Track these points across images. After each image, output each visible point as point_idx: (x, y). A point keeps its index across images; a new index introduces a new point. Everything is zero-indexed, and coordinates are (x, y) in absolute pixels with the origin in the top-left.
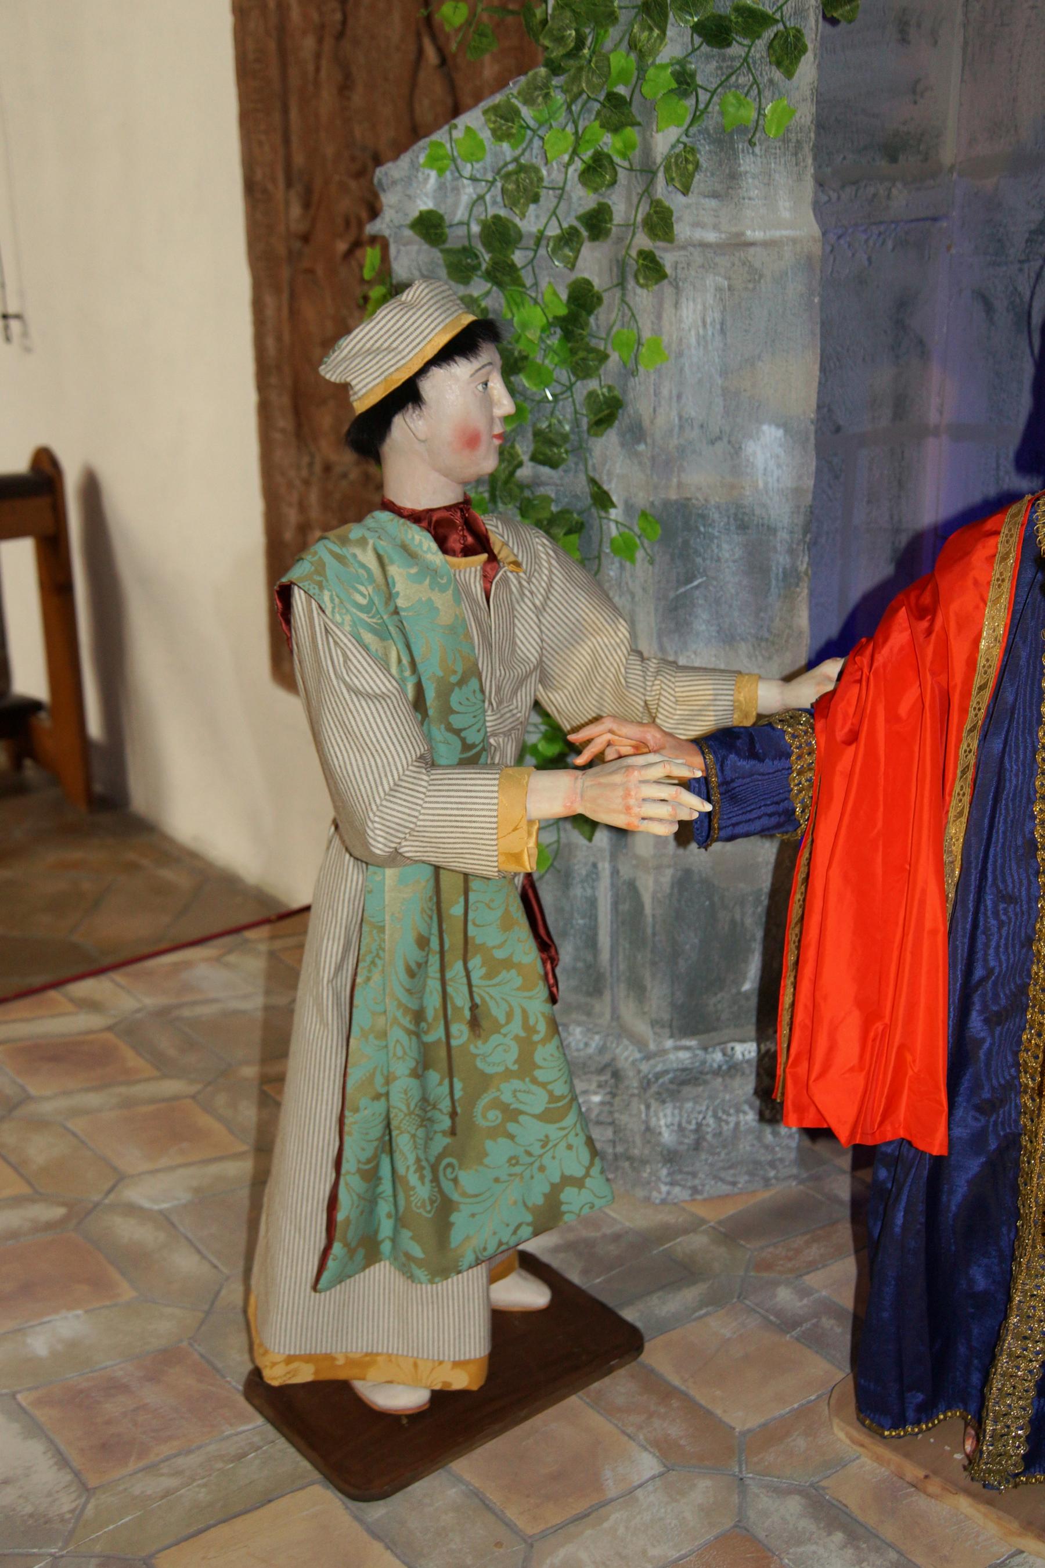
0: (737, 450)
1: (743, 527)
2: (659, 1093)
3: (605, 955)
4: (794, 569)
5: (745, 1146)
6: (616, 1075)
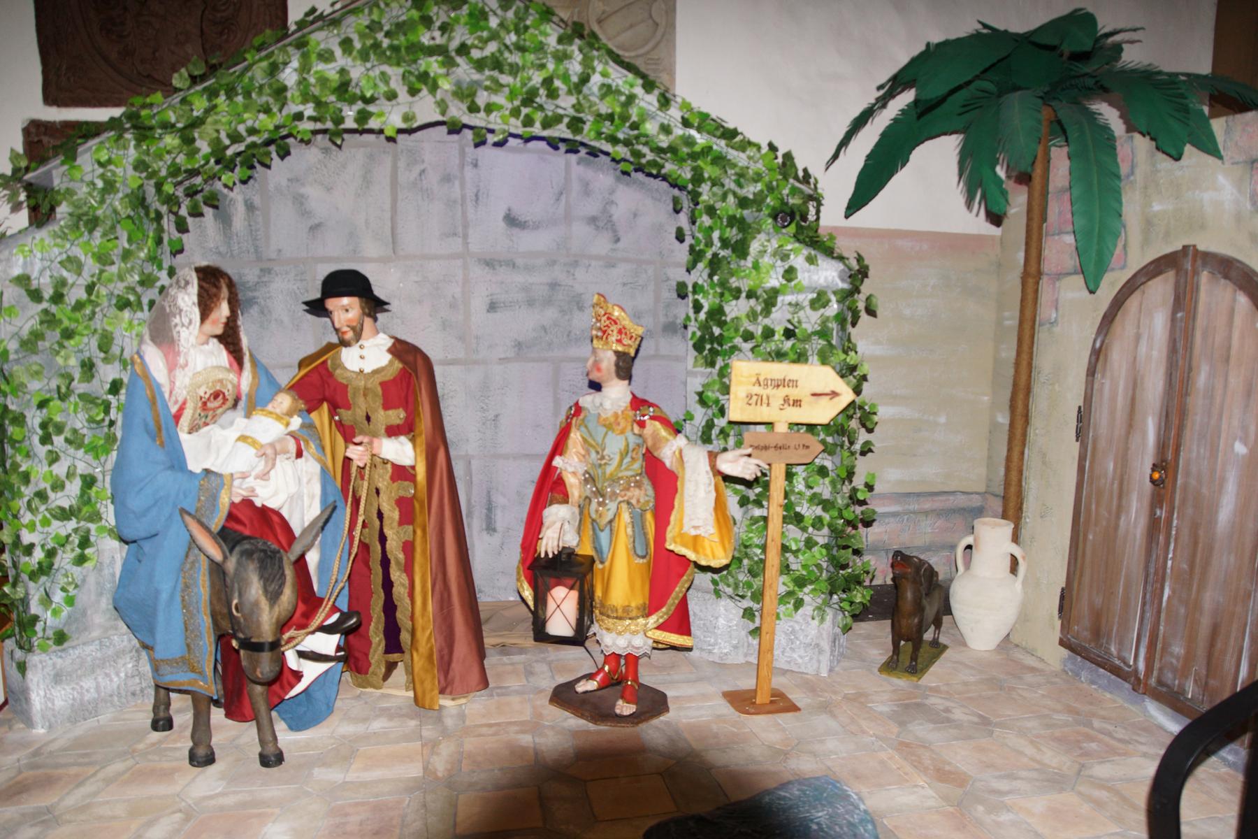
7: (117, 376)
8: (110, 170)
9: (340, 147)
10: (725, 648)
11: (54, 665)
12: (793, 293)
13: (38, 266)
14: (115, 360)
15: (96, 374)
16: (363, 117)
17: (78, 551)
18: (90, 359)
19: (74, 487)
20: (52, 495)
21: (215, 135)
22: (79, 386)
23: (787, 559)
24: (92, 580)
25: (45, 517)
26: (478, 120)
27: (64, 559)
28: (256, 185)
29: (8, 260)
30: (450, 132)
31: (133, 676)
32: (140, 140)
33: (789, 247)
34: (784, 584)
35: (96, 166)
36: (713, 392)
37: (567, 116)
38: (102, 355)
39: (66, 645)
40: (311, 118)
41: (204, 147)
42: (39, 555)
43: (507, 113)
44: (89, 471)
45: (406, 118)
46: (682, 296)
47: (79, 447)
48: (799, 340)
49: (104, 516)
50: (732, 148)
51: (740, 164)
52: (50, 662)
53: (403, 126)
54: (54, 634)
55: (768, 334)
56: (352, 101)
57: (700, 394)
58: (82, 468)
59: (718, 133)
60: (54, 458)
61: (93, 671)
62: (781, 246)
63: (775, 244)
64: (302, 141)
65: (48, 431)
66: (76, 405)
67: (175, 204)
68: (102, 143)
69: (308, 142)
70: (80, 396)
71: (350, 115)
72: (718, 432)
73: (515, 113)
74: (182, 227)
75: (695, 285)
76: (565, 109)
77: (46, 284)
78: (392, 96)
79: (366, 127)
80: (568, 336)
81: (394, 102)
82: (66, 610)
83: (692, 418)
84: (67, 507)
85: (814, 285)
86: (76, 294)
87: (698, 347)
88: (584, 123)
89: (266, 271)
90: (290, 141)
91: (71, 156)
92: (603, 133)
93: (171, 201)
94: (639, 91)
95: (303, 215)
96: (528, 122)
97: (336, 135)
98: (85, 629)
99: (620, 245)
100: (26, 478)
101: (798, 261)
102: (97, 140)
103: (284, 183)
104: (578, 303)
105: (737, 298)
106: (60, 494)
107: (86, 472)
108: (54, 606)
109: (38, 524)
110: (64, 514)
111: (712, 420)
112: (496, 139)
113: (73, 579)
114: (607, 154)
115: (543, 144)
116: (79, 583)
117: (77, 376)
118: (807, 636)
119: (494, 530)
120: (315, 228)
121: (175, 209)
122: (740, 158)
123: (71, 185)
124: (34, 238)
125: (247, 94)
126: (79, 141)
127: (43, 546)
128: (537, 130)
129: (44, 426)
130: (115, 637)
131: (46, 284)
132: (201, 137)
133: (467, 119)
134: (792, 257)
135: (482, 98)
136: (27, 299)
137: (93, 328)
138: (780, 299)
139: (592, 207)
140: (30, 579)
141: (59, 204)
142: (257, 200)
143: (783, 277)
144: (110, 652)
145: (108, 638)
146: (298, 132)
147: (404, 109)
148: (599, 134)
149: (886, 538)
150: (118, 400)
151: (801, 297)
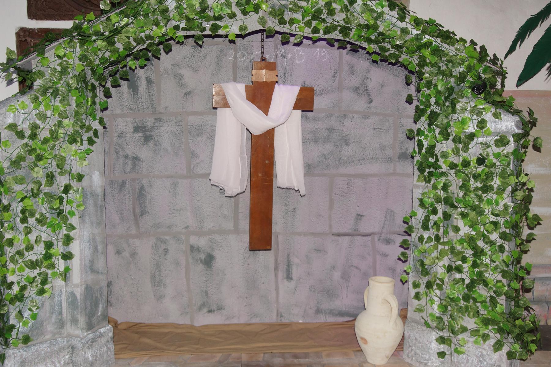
0: (91, 177)
1: (93, 196)
2: (88, 347)
3: (64, 316)
4: (102, 205)
5: (105, 357)
6: (73, 348)
7: (68, 183)
8: (65, 61)
9: (201, 46)
10: (436, 363)
11: (21, 355)
12: (483, 136)
13: (22, 117)
14: (67, 173)
15: (55, 181)
16: (215, 28)
17: (40, 286)
18: (51, 172)
19: (40, 250)
20: (26, 254)
21: (127, 40)
22: (45, 188)
23: (478, 307)
24: (47, 304)
25: (21, 266)
26: (285, 29)
27: (31, 292)
28: (153, 68)
29: (5, 114)
30: (268, 37)
31: (68, 364)
32: (82, 44)
33: (481, 107)
34: (475, 323)
35: (57, 58)
36: (429, 198)
37: (339, 26)
38: (59, 170)
39: (29, 344)
40: (183, 29)
41: (120, 46)
42: (16, 289)
43: (303, 25)
44: (49, 239)
45: (242, 28)
46: (410, 138)
47: (43, 225)
48: (486, 166)
49: (57, 266)
50: (445, 43)
51: (450, 54)
52: (19, 354)
53: (240, 33)
54: (23, 337)
55: (466, 164)
56: (208, 19)
57: (421, 200)
58: (44, 237)
59: (436, 34)
60: (28, 231)
61: (44, 360)
62: (476, 106)
63: (473, 104)
64: (178, 42)
65: (25, 215)
66: (43, 200)
67: (104, 80)
68: (60, 44)
69: (181, 43)
70: (45, 194)
71: (208, 25)
72: (432, 224)
73: (308, 24)
74: (108, 95)
75: (419, 131)
76: (338, 22)
77: (25, 127)
78: (232, 16)
79: (217, 34)
80: (339, 160)
81: (234, 19)
82: (31, 322)
83: (415, 215)
84: (35, 261)
85: (498, 131)
86: (44, 134)
87: (421, 170)
88: (351, 30)
89: (158, 120)
90: (172, 42)
91: (42, 53)
92: (362, 36)
93: (101, 79)
94: (386, 9)
95: (180, 86)
96: (316, 30)
97: (198, 41)
98: (42, 334)
99: (373, 104)
100: (11, 243)
101: (488, 116)
102: (57, 43)
103: (170, 67)
104: (346, 140)
105: (447, 139)
106: (31, 253)
107: (47, 240)
108: (24, 320)
109: (16, 270)
110: (33, 265)
111: (428, 216)
112: (296, 42)
113: (36, 304)
114: (364, 49)
115: (324, 43)
116: (40, 306)
117: (44, 183)
118: (491, 359)
119: (291, 279)
120: (187, 94)
121: (103, 84)
122: (450, 50)
123: (42, 69)
124: (18, 101)
125: (146, 16)
126: (47, 43)
127: (18, 283)
128: (321, 35)
129: (23, 212)
130: (60, 339)
131: (25, 127)
132: (119, 41)
133: (277, 28)
134: (484, 113)
135: (288, 16)
136: (15, 137)
137: (54, 154)
138: (475, 139)
139: (355, 81)
140: (10, 303)
141: (35, 80)
142: (153, 77)
143: (477, 126)
144: (56, 348)
145: (55, 339)
146: (177, 37)
147: (240, 23)
148: (360, 36)
149: (547, 294)
150: (68, 197)
151: (489, 139)
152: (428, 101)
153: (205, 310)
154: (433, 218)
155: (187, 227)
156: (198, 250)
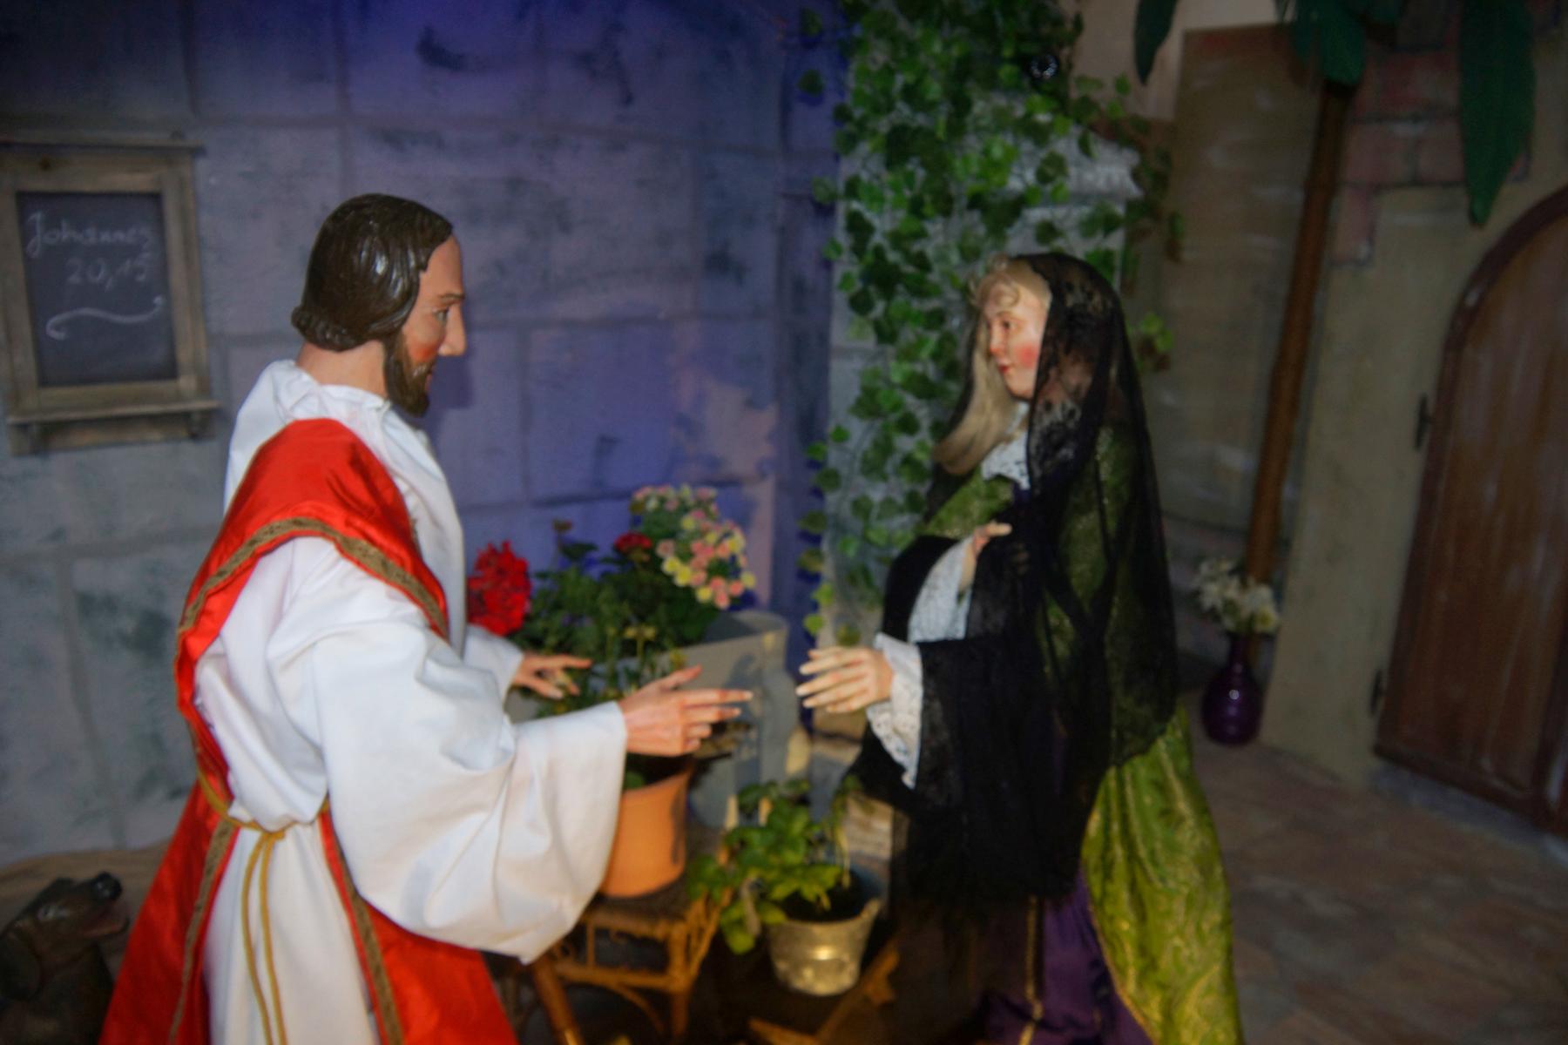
33: (1043, 118)
62: (1029, 115)
63: (1020, 112)
87: (860, 304)
134: (1052, 137)
151: (1060, 212)
152: (886, 93)
153: (160, 793)
154: (905, 443)
155: (58, 535)
156: (110, 604)
